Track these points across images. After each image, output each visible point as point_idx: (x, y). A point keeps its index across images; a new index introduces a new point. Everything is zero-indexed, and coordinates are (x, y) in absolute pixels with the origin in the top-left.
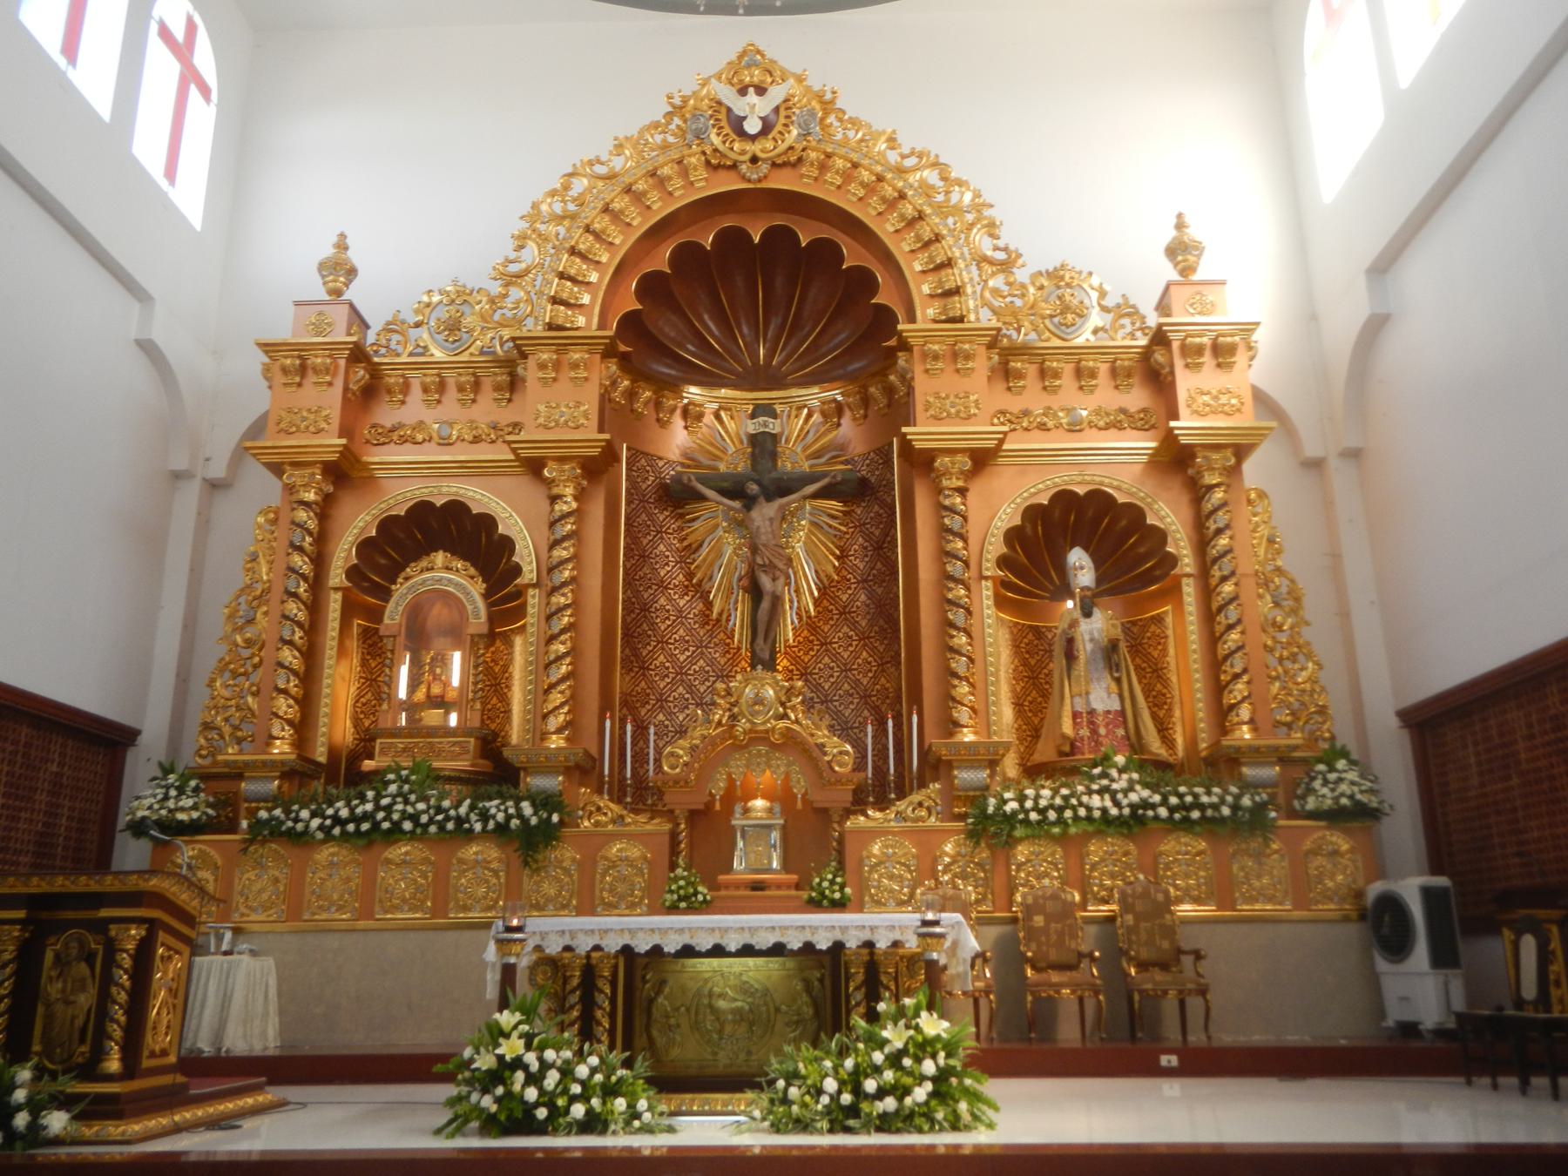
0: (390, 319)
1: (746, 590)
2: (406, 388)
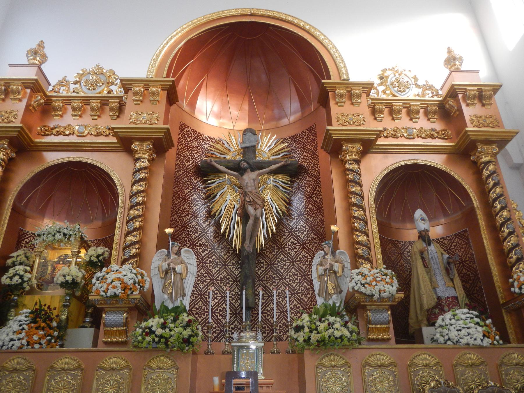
0: (61, 79)
1: (240, 216)
2: (63, 110)
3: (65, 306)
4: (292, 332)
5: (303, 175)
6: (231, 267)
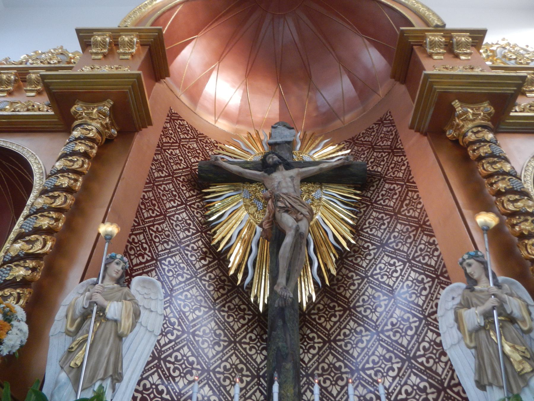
5: (377, 185)
6: (248, 347)
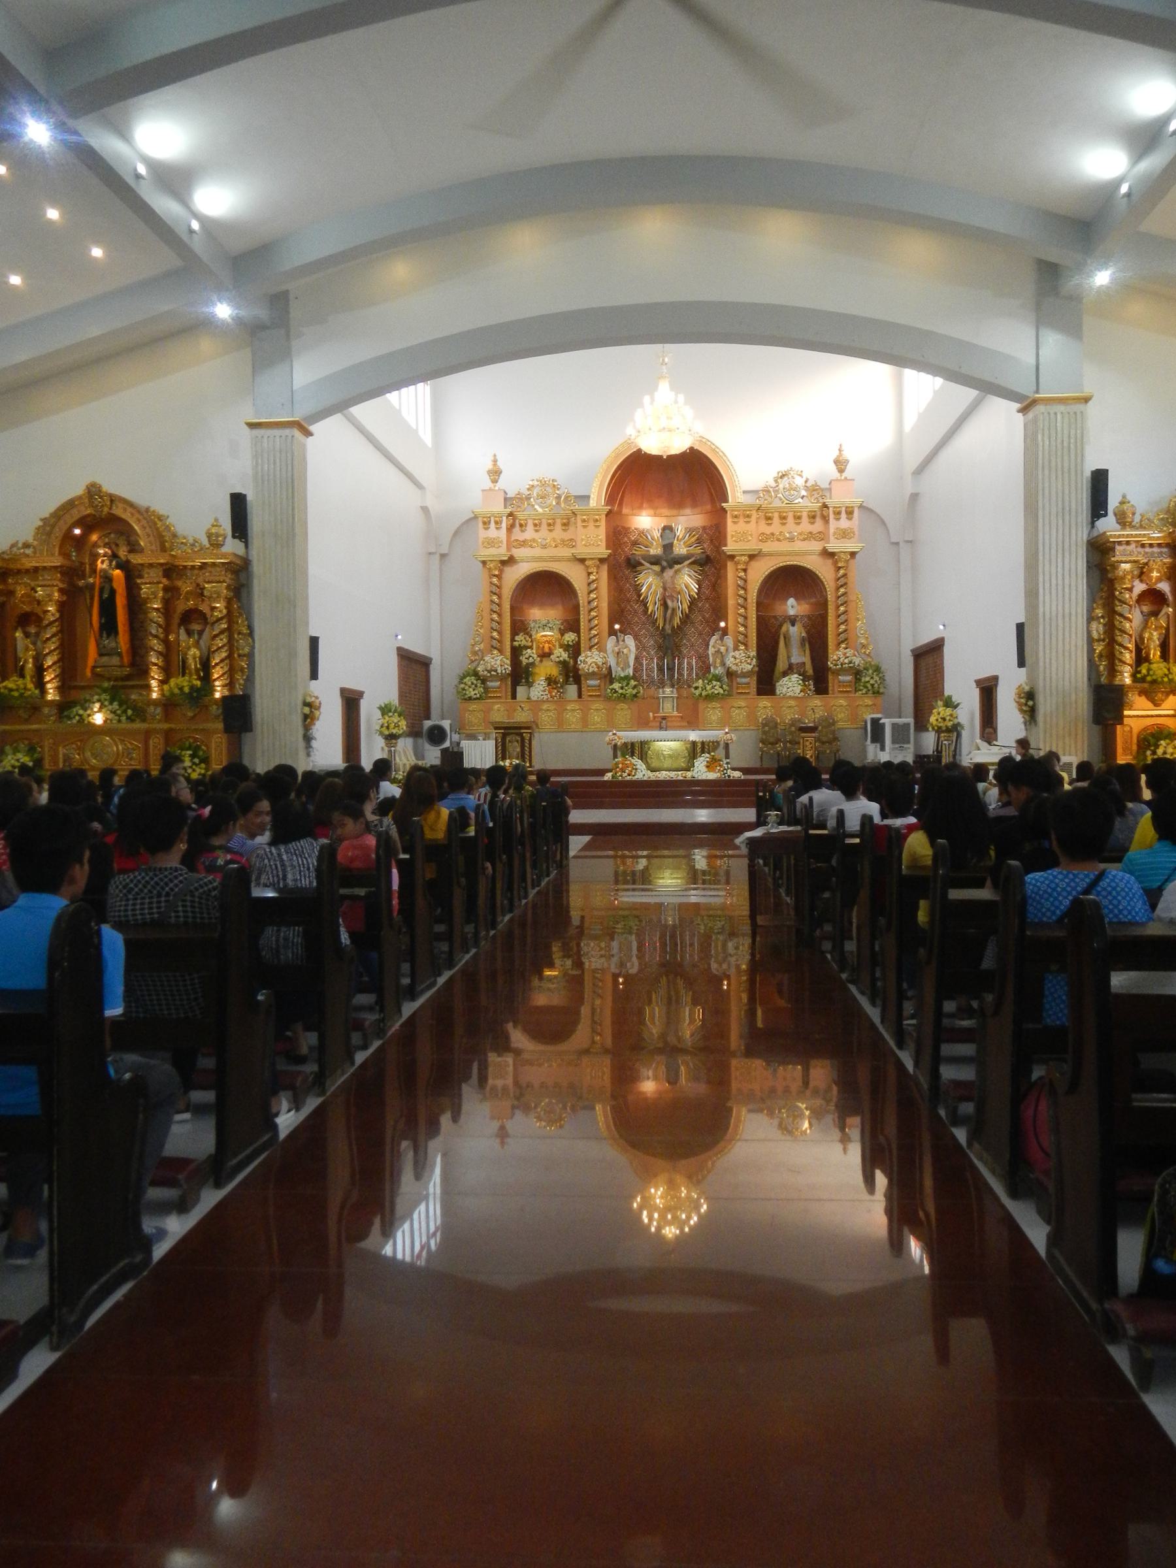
3: (561, 674)
4: (693, 690)
